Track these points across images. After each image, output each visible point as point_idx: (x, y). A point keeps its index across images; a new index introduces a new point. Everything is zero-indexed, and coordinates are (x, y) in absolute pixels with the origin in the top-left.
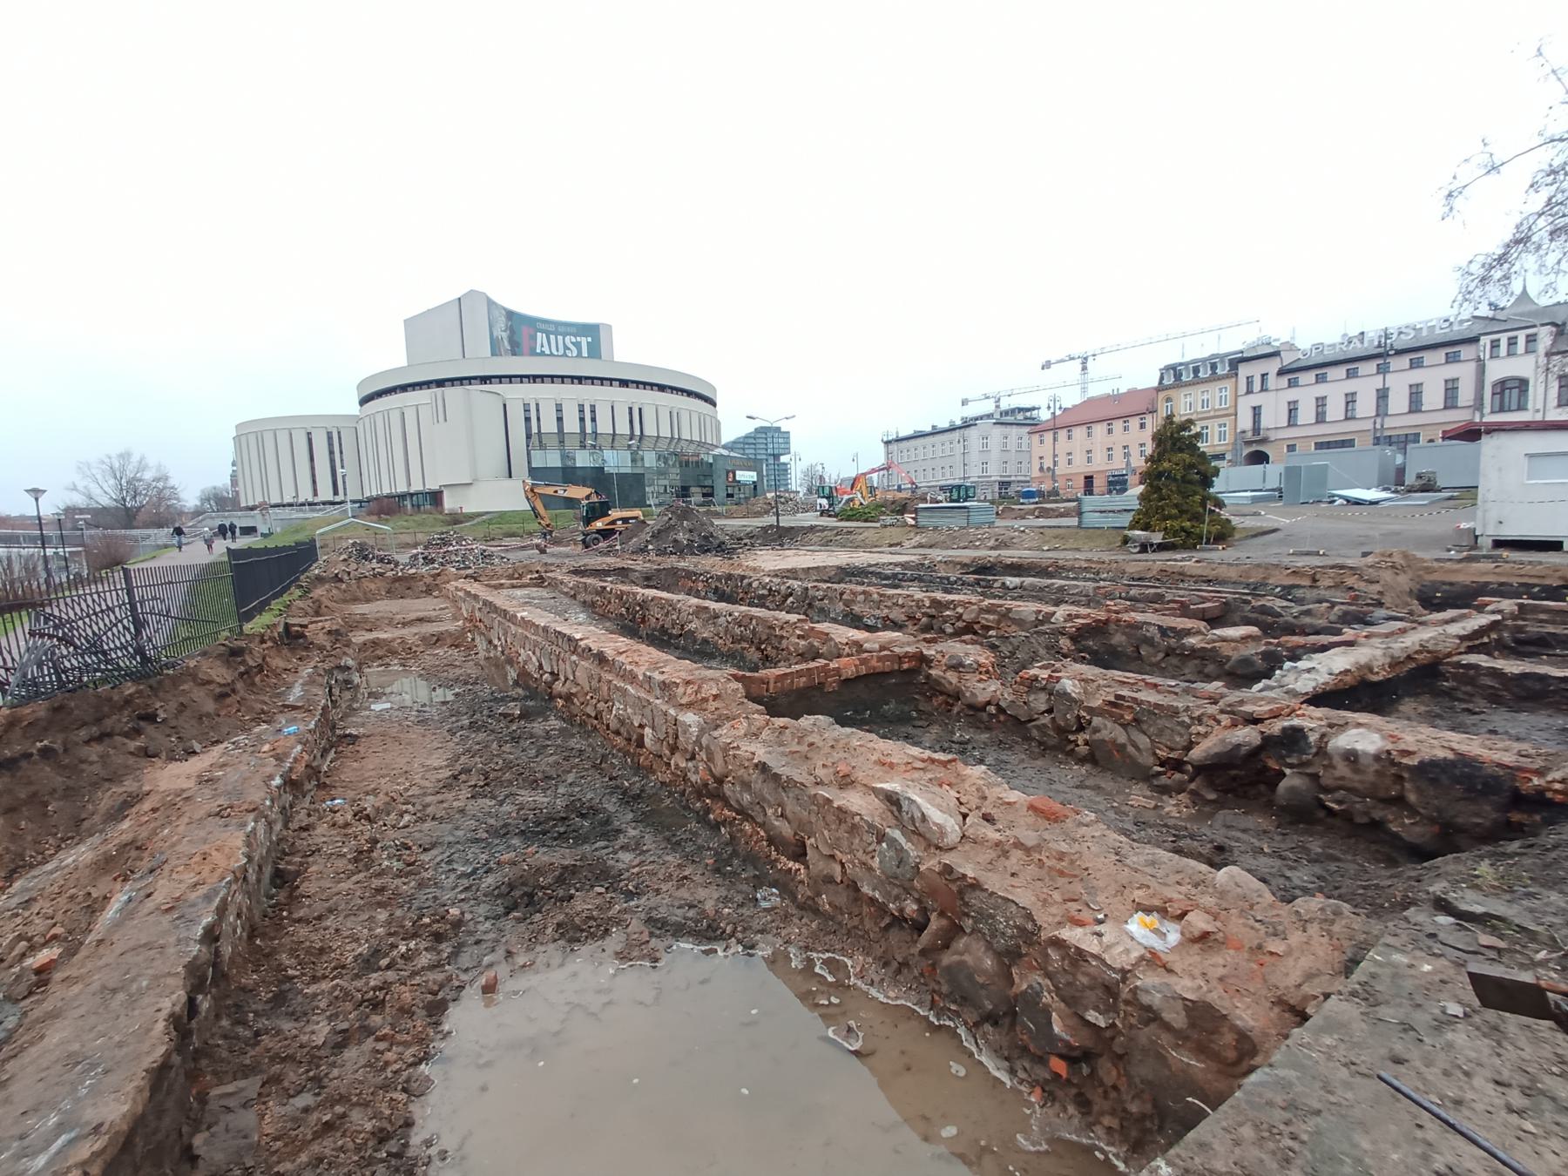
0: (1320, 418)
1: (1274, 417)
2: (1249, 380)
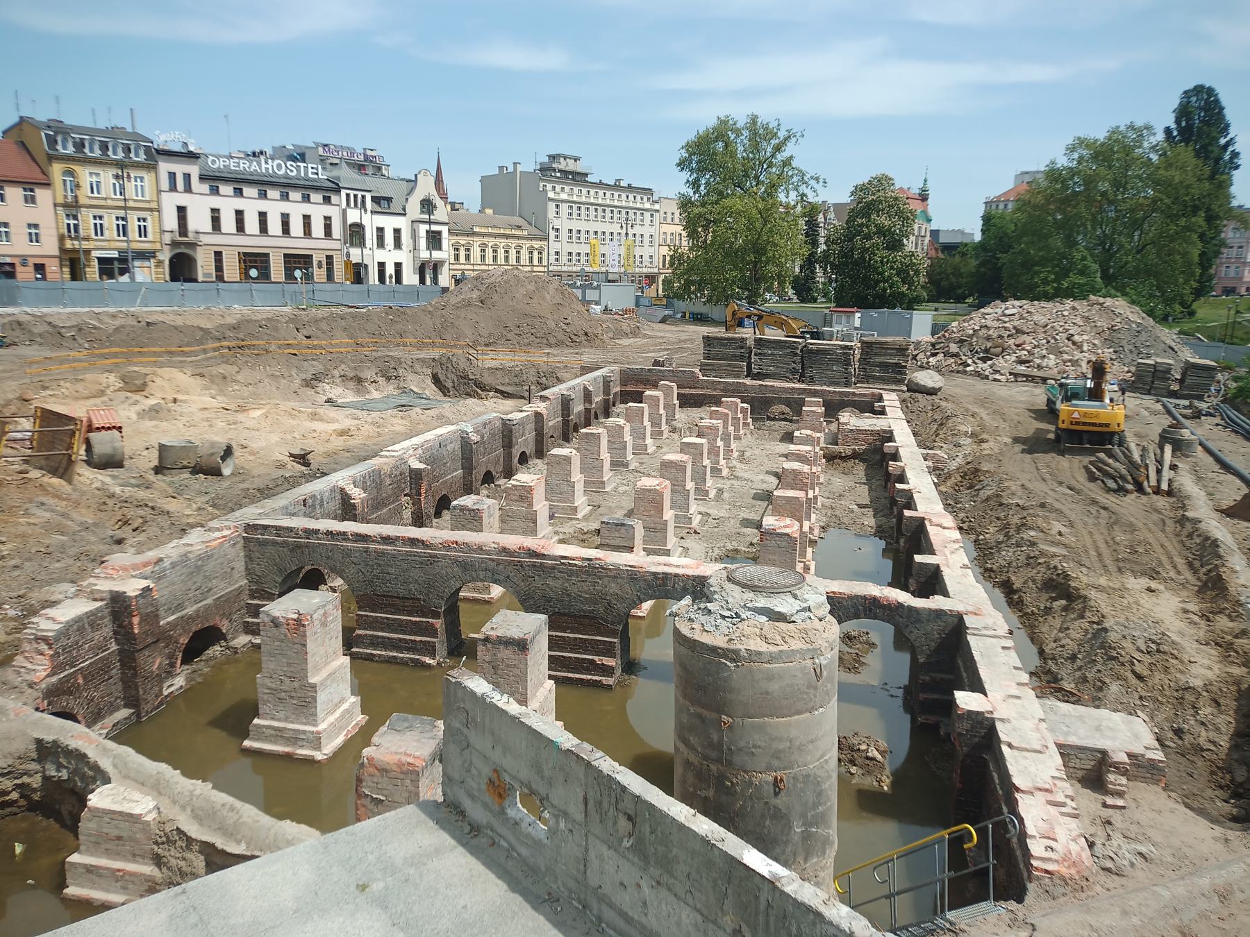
0: (240, 227)
1: (199, 221)
2: (172, 176)
